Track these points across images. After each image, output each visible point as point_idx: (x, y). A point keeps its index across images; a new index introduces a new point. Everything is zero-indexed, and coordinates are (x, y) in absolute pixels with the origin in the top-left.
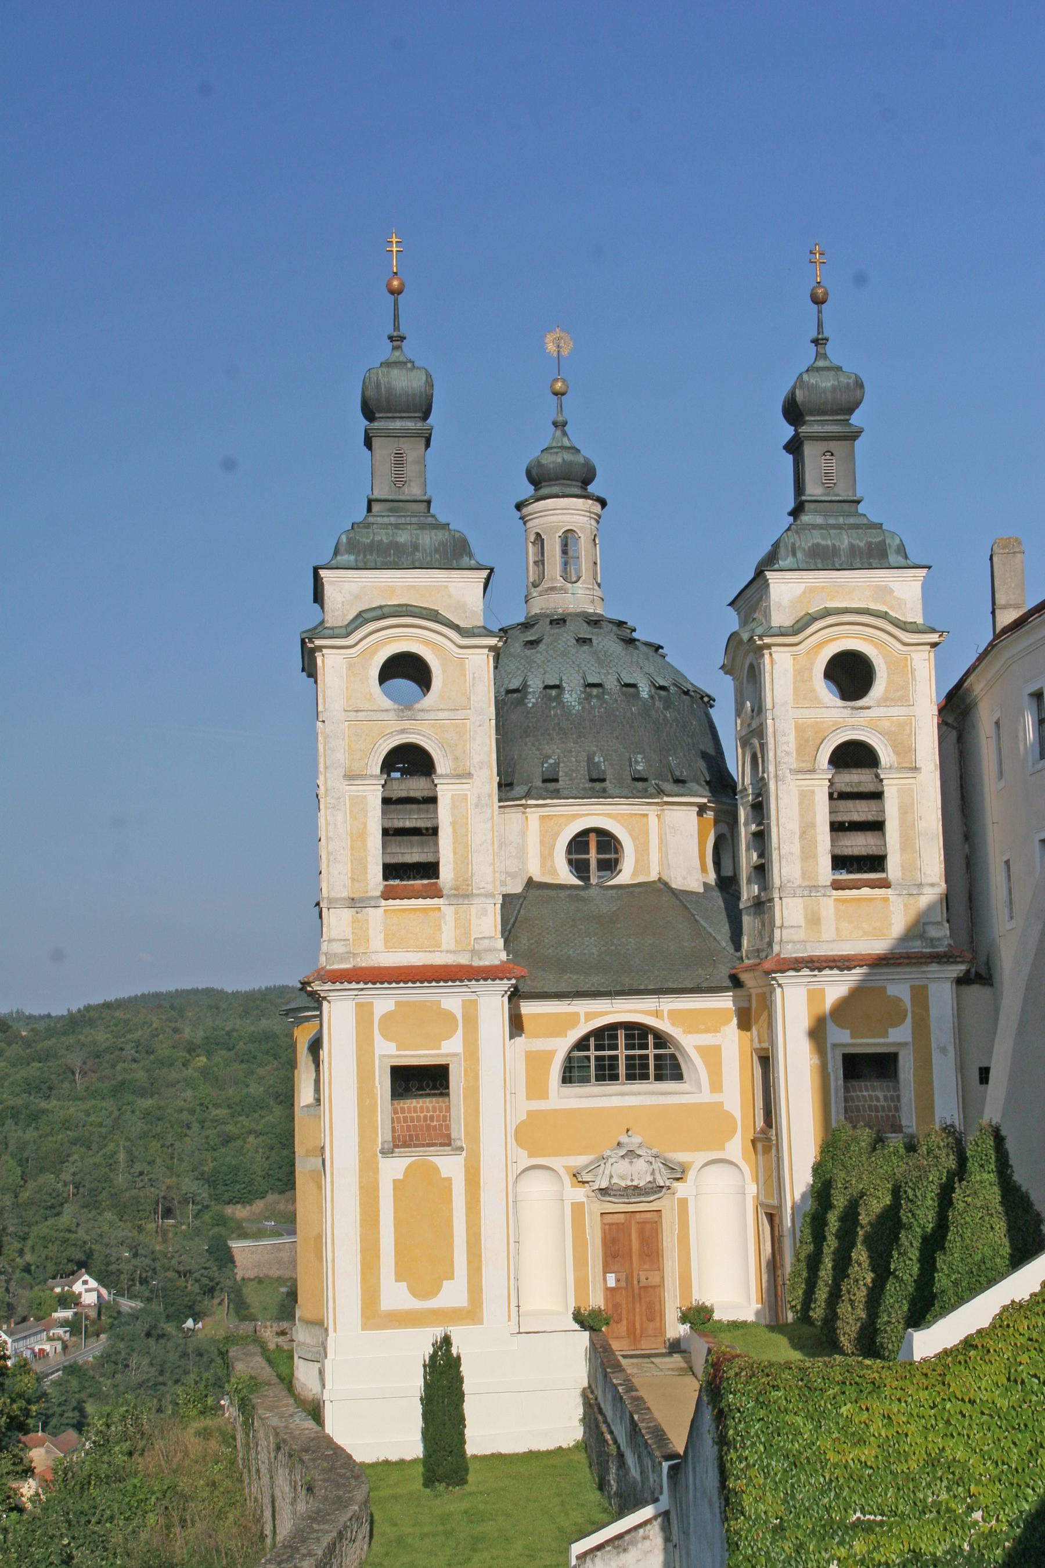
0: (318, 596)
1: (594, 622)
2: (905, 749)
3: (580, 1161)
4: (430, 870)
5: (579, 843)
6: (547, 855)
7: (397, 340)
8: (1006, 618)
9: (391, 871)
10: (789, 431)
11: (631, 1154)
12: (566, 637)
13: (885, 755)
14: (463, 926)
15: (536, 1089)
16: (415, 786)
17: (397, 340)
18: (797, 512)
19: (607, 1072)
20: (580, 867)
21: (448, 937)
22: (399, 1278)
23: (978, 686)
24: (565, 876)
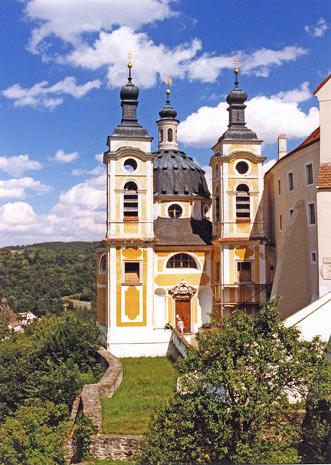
0: (108, 144)
1: (175, 152)
2: (256, 186)
3: (171, 287)
4: (136, 214)
5: (171, 208)
6: (163, 211)
7: (130, 79)
8: (282, 155)
9: (126, 214)
10: (228, 106)
11: (183, 286)
12: (169, 156)
13: (251, 190)
14: (143, 231)
15: (160, 269)
16: (133, 192)
17: (130, 79)
18: (229, 126)
19: (178, 266)
20: (171, 214)
21: (140, 231)
22: (126, 314)
23: (274, 172)
24: (167, 216)
